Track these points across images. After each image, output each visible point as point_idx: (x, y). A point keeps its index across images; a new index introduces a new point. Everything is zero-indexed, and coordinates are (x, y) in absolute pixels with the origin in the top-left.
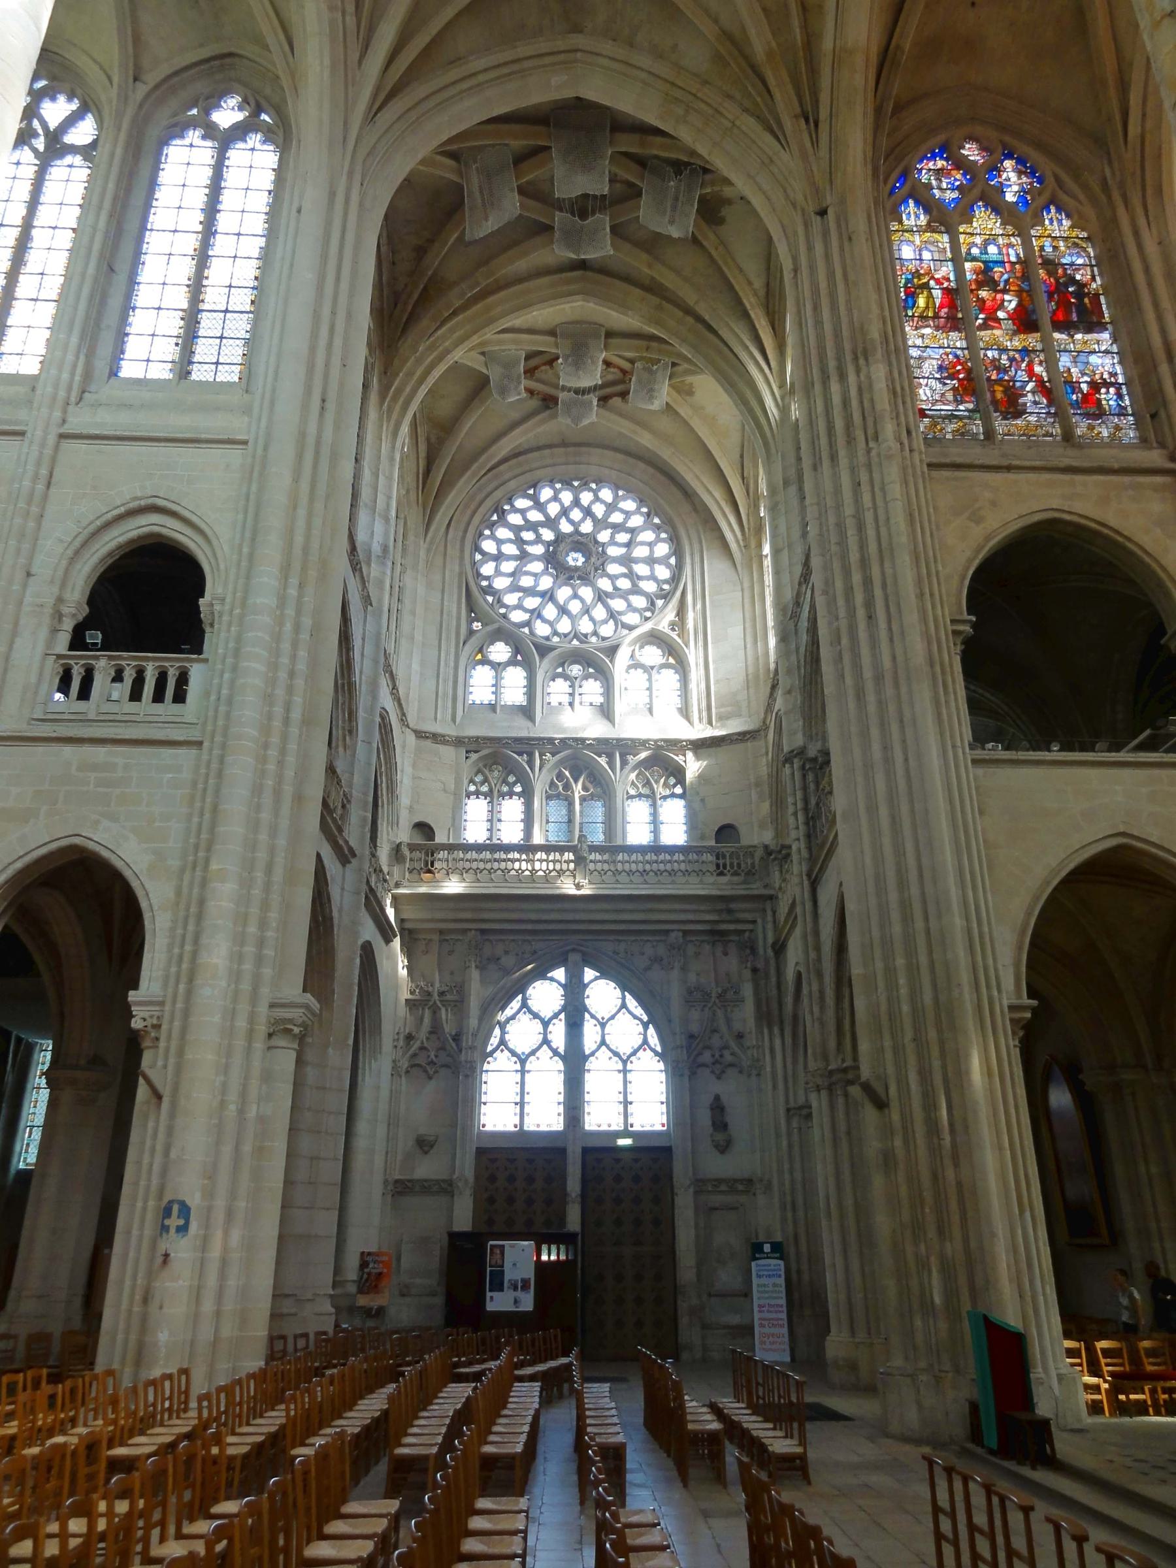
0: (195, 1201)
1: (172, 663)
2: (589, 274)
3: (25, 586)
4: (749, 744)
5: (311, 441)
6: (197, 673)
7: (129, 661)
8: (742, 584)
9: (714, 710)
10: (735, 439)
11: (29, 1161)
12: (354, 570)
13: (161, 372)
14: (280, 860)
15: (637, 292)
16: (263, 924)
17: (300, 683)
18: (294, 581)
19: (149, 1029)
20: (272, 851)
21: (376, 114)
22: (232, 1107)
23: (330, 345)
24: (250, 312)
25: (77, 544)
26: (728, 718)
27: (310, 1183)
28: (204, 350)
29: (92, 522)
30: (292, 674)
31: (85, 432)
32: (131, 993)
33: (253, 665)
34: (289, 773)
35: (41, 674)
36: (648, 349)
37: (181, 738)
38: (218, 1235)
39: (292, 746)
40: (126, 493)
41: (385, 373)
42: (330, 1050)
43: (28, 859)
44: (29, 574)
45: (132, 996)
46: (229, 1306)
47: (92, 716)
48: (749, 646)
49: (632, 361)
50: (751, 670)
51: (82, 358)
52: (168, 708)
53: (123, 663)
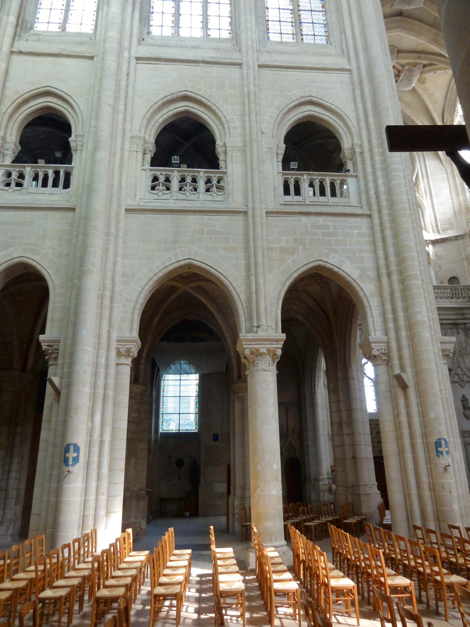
2: (404, 18)
4: (460, 241)
8: (446, 170)
9: (440, 227)
10: (441, 104)
11: (164, 429)
15: (427, 27)
19: (380, 355)
24: (322, 11)
26: (447, 230)
31: (271, 64)
36: (419, 58)
48: (454, 198)
49: (403, 66)
50: (456, 208)
53: (314, 177)
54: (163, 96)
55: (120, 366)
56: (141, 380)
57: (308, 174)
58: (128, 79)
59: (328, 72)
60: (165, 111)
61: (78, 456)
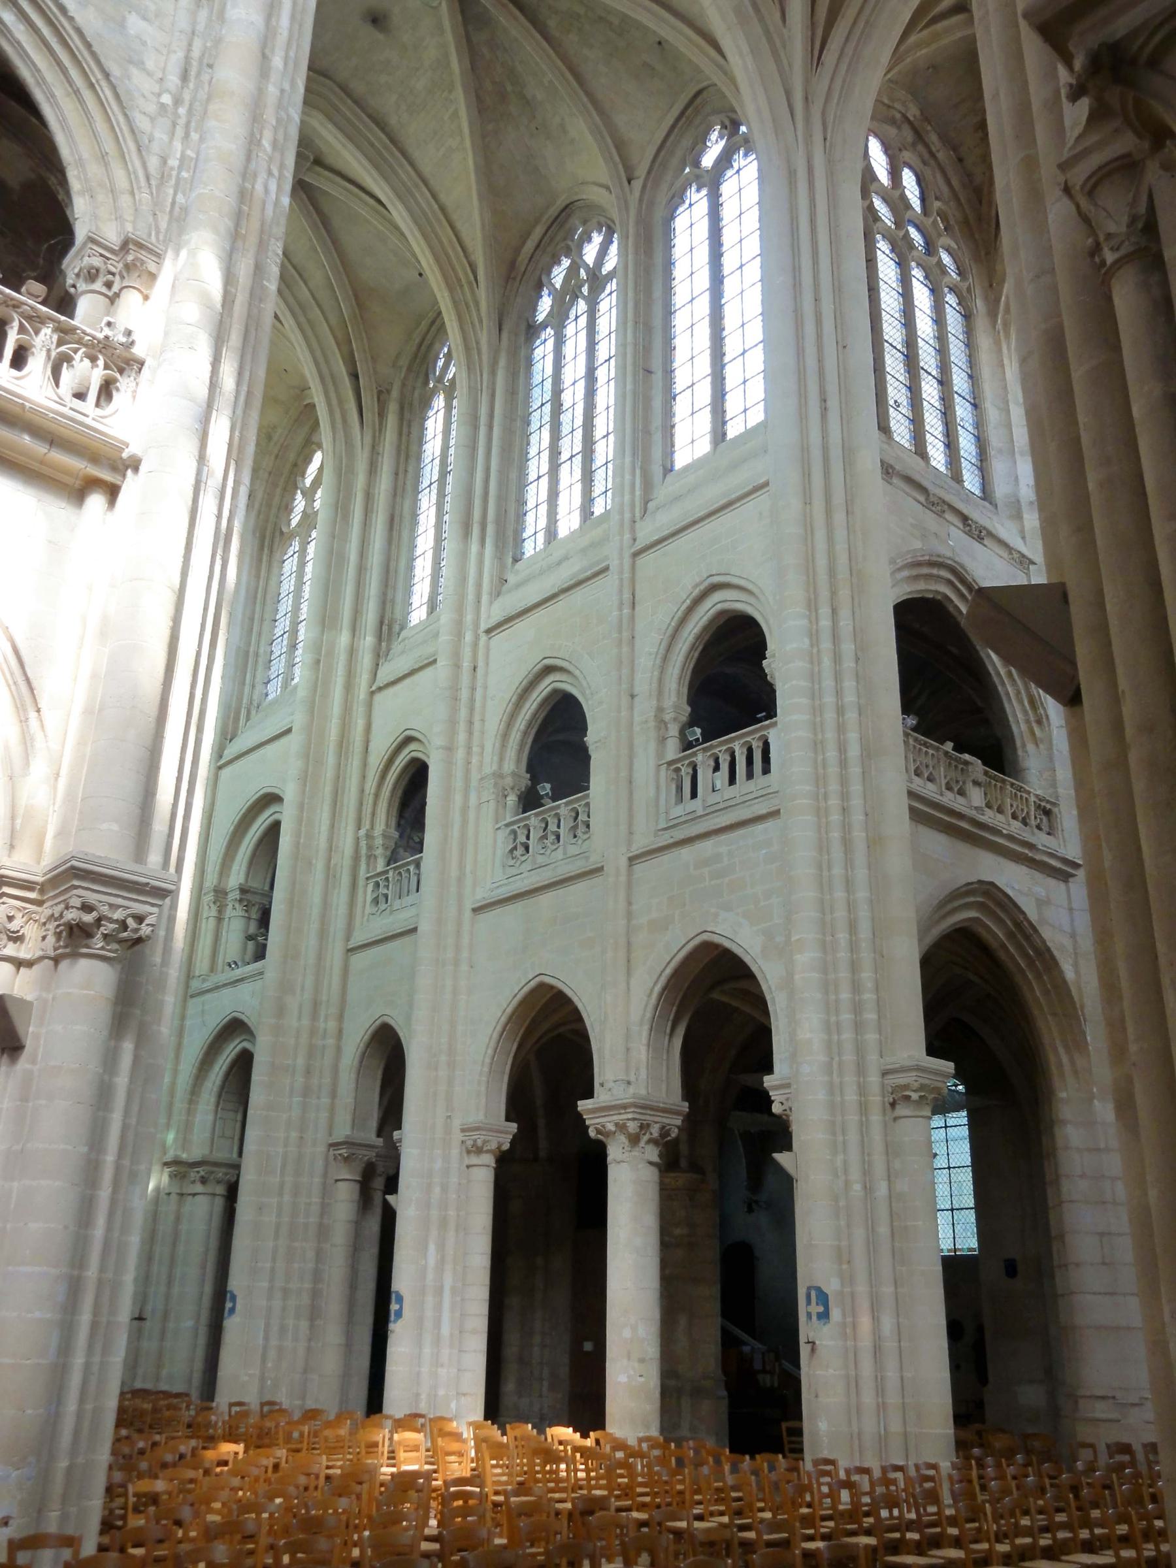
0: (832, 1286)
1: (750, 736)
3: (631, 708)
5: (816, 454)
6: (773, 736)
7: (719, 747)
12: (980, 539)
13: (704, 447)
14: (864, 913)
16: (856, 988)
17: (851, 716)
18: (825, 611)
20: (851, 906)
21: (819, 58)
22: (857, 1187)
23: (819, 336)
25: (662, 651)
27: (1104, 1264)
28: (733, 405)
29: (669, 624)
30: (840, 710)
32: (766, 1078)
33: (795, 717)
34: (858, 817)
35: (658, 788)
37: (764, 811)
38: (865, 1322)
39: (856, 788)
40: (688, 583)
41: (991, 286)
42: (1095, 1101)
43: (673, 964)
44: (632, 696)
45: (768, 1081)
46: (893, 1399)
47: (700, 812)
51: (638, 472)
52: (760, 780)
53: (716, 751)
54: (517, 684)
55: (471, 1169)
56: (683, 1163)
57: (703, 749)
58: (474, 678)
59: (738, 505)
60: (527, 705)
61: (401, 1308)
